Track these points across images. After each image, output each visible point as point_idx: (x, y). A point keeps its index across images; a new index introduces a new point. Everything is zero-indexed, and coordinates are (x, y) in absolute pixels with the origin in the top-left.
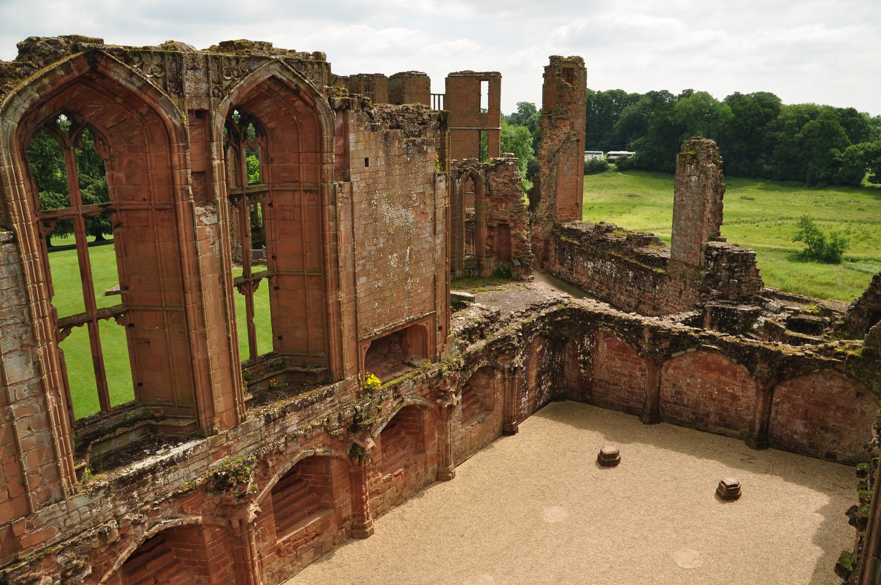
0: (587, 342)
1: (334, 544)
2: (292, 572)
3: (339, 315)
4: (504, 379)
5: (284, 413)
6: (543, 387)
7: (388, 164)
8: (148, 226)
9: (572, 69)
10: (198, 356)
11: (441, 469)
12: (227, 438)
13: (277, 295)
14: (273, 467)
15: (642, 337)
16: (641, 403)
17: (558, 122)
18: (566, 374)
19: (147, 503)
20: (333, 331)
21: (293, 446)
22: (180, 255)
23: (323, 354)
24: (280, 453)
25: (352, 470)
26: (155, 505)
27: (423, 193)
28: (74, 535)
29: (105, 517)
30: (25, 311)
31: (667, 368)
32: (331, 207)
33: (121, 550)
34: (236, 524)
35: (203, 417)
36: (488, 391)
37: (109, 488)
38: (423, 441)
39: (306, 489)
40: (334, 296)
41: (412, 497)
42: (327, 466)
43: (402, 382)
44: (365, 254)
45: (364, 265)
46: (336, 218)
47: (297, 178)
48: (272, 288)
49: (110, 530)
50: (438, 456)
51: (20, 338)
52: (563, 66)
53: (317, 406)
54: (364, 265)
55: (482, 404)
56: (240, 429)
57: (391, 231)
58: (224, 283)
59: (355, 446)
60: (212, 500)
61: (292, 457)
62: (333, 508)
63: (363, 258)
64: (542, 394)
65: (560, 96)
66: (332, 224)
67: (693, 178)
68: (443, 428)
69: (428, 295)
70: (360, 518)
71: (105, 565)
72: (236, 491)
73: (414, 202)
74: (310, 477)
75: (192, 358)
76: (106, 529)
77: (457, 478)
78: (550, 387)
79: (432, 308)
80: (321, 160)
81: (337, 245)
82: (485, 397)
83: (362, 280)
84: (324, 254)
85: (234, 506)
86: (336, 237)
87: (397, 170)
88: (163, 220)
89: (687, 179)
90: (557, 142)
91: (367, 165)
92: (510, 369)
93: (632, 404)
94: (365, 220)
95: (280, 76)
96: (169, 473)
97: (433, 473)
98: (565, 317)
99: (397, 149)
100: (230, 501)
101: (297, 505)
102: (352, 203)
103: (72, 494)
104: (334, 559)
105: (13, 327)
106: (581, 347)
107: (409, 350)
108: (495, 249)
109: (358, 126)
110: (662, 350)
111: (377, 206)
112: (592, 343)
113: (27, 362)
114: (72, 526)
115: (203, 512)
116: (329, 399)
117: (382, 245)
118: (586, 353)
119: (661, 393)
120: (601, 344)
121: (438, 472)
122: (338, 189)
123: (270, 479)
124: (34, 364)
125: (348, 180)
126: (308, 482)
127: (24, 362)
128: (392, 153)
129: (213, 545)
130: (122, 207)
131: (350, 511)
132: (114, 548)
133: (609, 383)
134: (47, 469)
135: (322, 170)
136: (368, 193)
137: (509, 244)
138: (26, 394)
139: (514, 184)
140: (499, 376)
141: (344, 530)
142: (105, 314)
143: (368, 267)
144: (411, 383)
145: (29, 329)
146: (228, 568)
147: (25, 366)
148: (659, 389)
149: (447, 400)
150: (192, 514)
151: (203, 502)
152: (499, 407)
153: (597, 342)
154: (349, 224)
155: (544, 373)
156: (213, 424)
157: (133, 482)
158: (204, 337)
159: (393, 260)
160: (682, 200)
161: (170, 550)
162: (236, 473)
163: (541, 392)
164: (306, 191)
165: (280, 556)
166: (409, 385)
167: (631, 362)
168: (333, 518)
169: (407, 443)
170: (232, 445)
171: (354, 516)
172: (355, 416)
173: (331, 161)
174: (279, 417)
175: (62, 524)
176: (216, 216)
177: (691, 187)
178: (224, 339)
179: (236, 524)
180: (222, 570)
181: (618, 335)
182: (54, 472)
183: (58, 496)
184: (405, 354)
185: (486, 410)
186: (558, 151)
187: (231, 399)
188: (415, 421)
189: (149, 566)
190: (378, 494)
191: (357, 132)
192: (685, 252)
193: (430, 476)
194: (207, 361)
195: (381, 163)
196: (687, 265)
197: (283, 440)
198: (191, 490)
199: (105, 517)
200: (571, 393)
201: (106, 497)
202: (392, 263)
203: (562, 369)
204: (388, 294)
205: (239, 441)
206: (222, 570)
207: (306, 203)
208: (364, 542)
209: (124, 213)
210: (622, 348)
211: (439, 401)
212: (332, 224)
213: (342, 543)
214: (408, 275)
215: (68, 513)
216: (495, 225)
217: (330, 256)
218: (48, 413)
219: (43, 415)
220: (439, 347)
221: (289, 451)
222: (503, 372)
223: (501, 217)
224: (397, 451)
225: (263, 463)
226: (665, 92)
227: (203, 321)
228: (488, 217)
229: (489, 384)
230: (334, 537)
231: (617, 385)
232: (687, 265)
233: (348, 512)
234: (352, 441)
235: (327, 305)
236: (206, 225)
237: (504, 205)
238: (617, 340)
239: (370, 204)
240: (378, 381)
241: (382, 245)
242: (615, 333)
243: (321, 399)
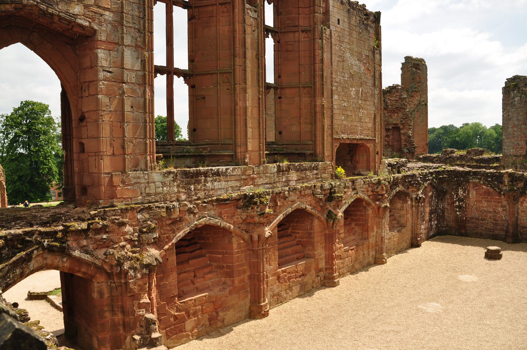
0: (461, 192)
1: (313, 288)
2: (285, 299)
3: (323, 114)
4: (412, 206)
5: (288, 169)
6: (433, 223)
8: (213, 16)
9: (418, 64)
10: (240, 104)
11: (378, 256)
12: (253, 171)
13: (280, 102)
14: (280, 206)
15: (502, 182)
16: (504, 230)
17: (413, 93)
18: (446, 217)
19: (199, 199)
20: (319, 124)
21: (293, 197)
22: (234, 31)
23: (310, 142)
24: (285, 198)
25: (327, 232)
26: (204, 202)
28: (150, 202)
29: (171, 197)
30: (142, 22)
31: (522, 203)
32: (320, 41)
33: (179, 230)
34: (256, 237)
35: (239, 150)
36: (402, 212)
37: (176, 175)
38: (367, 231)
39: (295, 242)
40: (320, 101)
41: (361, 270)
42: (312, 223)
43: (357, 179)
46: (322, 48)
47: (297, 24)
48: (277, 97)
49: (174, 207)
51: (136, 39)
52: (413, 62)
53: (308, 173)
55: (398, 222)
56: (262, 168)
58: (259, 59)
59: (330, 212)
60: (241, 215)
61: (292, 205)
62: (313, 258)
64: (432, 228)
65: (413, 79)
66: (320, 52)
67: (516, 99)
68: (379, 224)
69: (370, 125)
70: (330, 271)
71: (167, 237)
72: (259, 210)
74: (298, 233)
75: (236, 104)
76: (171, 206)
77: (388, 263)
78: (436, 225)
79: (373, 136)
80: (314, 10)
81: (323, 66)
82: (400, 217)
83: (336, 97)
84: (315, 71)
85: (255, 224)
86: (322, 60)
88: (223, 12)
89: (511, 101)
90: (413, 106)
91: (339, 24)
92: (416, 198)
93: (496, 232)
96: (215, 181)
97: (372, 257)
98: (445, 176)
100: (253, 217)
101: (289, 250)
102: (331, 43)
103: (152, 170)
104: (314, 296)
105: (133, 30)
106: (457, 196)
107: (358, 165)
108: (390, 144)
110: (518, 188)
112: (464, 192)
113: (138, 58)
114: (149, 195)
115: (234, 222)
116: (315, 172)
118: (460, 200)
119: (519, 221)
120: (471, 192)
121: (375, 258)
122: (324, 31)
123: (277, 216)
124: (142, 61)
125: (329, 28)
126: (296, 237)
127: (136, 56)
129: (238, 252)
130: (196, 5)
131: (324, 264)
132: (176, 222)
133: (479, 220)
134: (139, 142)
135: (314, 16)
137: (400, 140)
138: (134, 80)
139: (402, 101)
140: (409, 202)
141: (319, 278)
142: (179, 73)
144: (362, 183)
145: (142, 35)
146: (246, 276)
147: (136, 60)
148: (517, 218)
149: (383, 202)
150: (227, 221)
151: (234, 215)
152: (409, 225)
153: (468, 192)
154: (329, 56)
155: (433, 213)
156: (245, 158)
157: (192, 177)
158: (245, 90)
160: (509, 116)
161: (205, 256)
162: (260, 196)
163: (431, 225)
164: (302, 31)
165: (279, 282)
167: (494, 202)
168: (313, 266)
169: (356, 232)
170: (256, 179)
171: (326, 269)
172: (331, 189)
173: (319, 16)
174: (286, 171)
175: (143, 189)
176: (257, 14)
177: (515, 105)
178: (257, 98)
179: (256, 237)
181: (484, 184)
182: (142, 147)
183: (142, 166)
184: (355, 168)
185: (401, 226)
186: (414, 111)
187: (258, 144)
188: (362, 215)
189: (191, 262)
190: (341, 259)
192: (513, 148)
193: (371, 260)
194: (246, 109)
196: (516, 156)
197: (287, 188)
198: (228, 200)
199: (171, 197)
200: (453, 229)
201: (174, 181)
202: (352, 94)
203: (443, 213)
205: (260, 177)
207: (302, 39)
208: (334, 289)
210: (488, 193)
211: (377, 203)
212: (320, 52)
213: (318, 289)
215: (148, 183)
216: (391, 127)
217: (318, 73)
218: (145, 99)
219: (142, 100)
221: (290, 199)
222: (412, 200)
223: (394, 122)
224: (350, 235)
225: (274, 200)
226: (452, 126)
227: (245, 79)
228: (386, 123)
229: (403, 207)
230: (313, 282)
231: (484, 220)
232: (516, 156)
233: (322, 264)
234: (327, 208)
235: (315, 106)
236: (251, 17)
237: (396, 115)
238: (483, 188)
240: (343, 171)
242: (482, 182)
243: (311, 169)
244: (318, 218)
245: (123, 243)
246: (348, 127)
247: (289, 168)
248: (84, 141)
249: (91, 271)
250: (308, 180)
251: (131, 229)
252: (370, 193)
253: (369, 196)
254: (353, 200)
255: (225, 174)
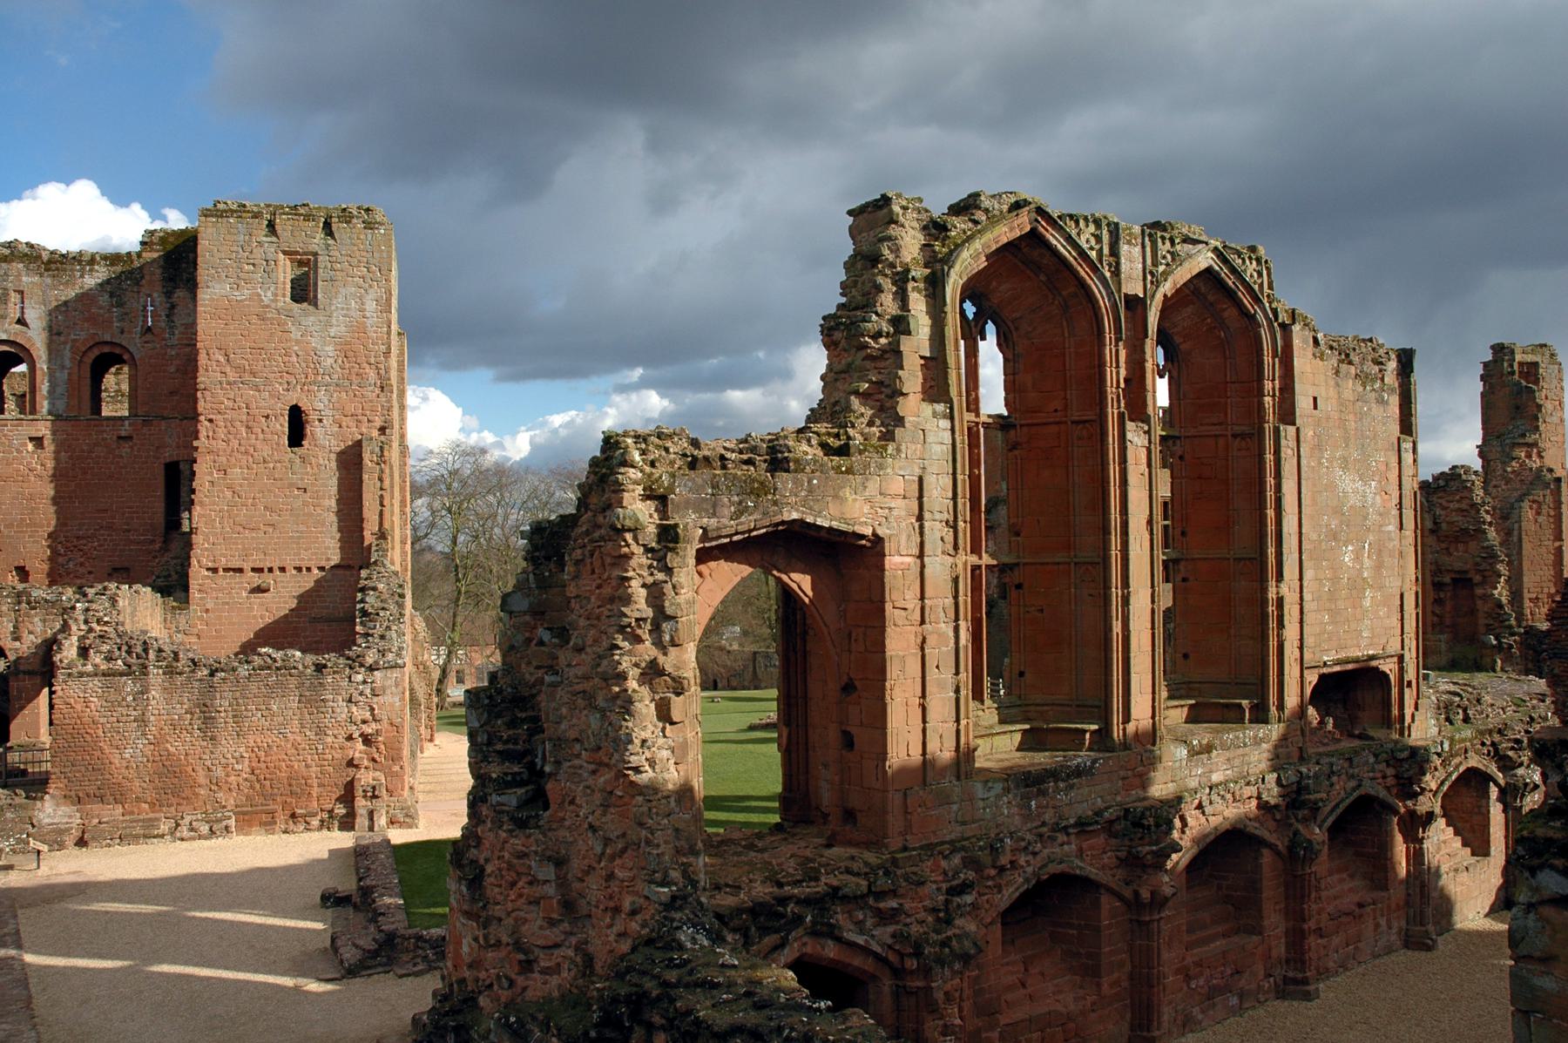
20: (1273, 643)
50: (1407, 903)
62: (1260, 933)
108: (1448, 621)
131: (1283, 949)
137: (1473, 612)
172: (1299, 783)
180: (1116, 975)
206: (1116, 975)
209: (1025, 429)
216: (1447, 579)
220: (1408, 712)
223: (1458, 565)
233: (1280, 950)
235: (1265, 602)
237: (1461, 547)
244: (1271, 846)
248: (854, 730)
249: (868, 965)
252: (1390, 781)
253: (1388, 788)
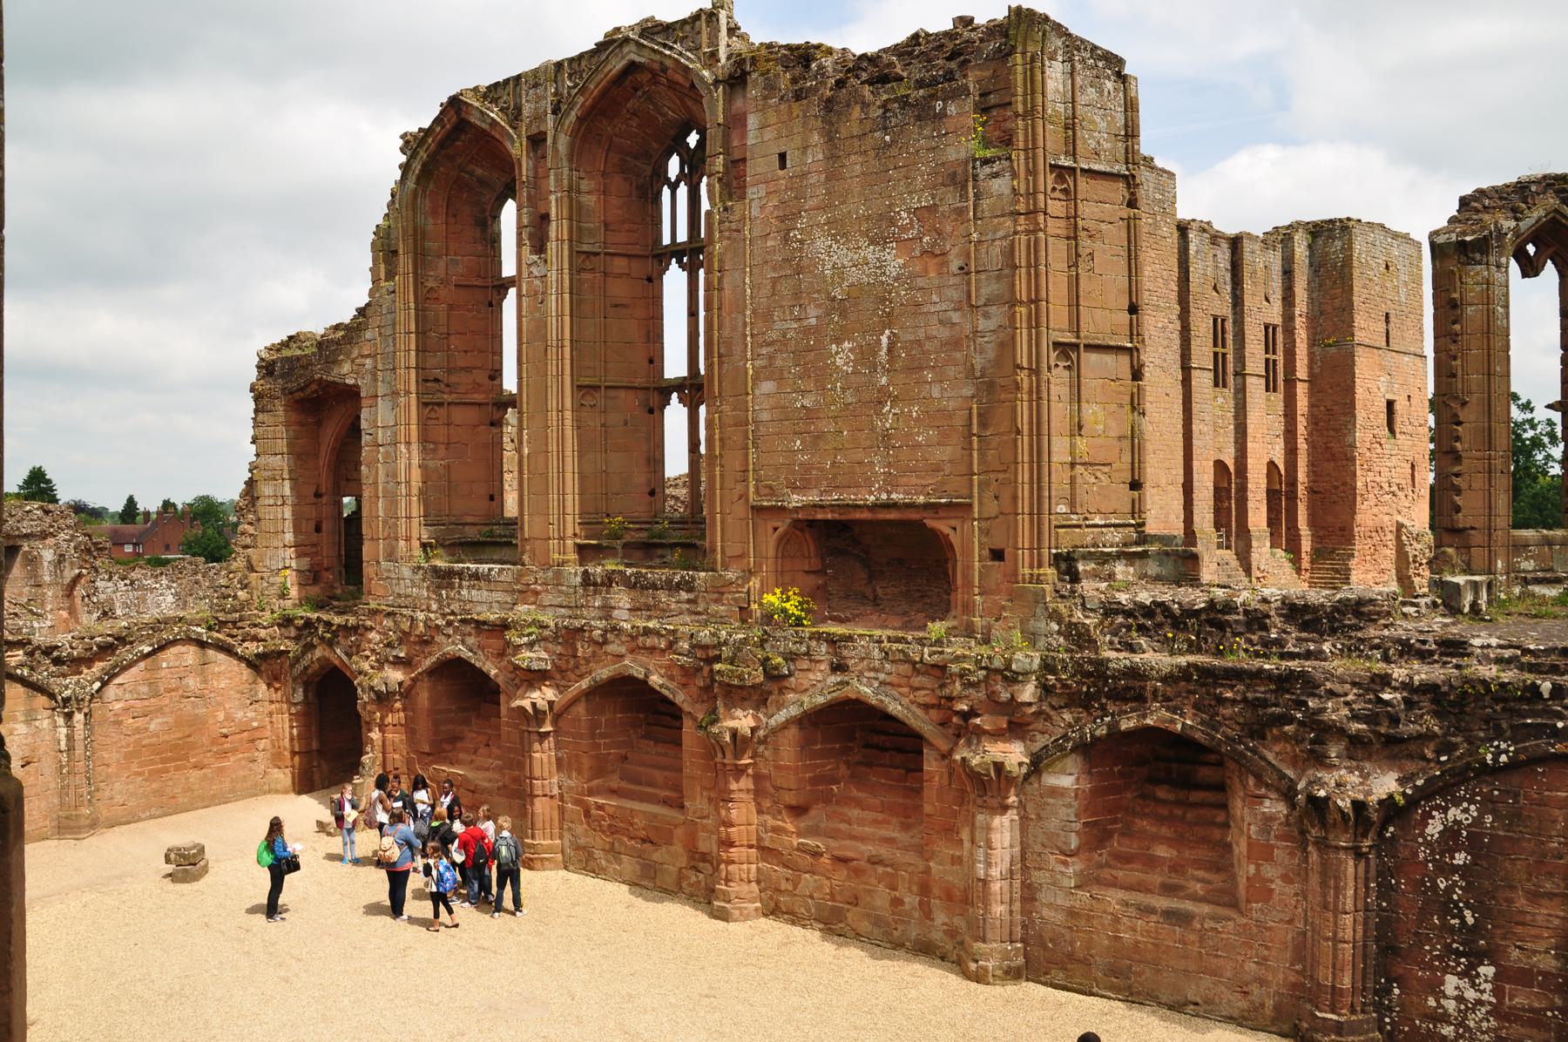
5: (609, 581)
7: (832, 157)
27: (932, 209)
43: (850, 638)
44: (774, 335)
45: (771, 358)
53: (663, 596)
54: (771, 358)
57: (838, 294)
63: (769, 344)
73: (904, 229)
87: (855, 166)
91: (783, 166)
94: (774, 269)
95: (638, 59)
96: (473, 587)
99: (855, 124)
109: (765, 98)
111: (802, 242)
114: (399, 595)
116: (684, 595)
117: (813, 321)
128: (844, 133)
136: (782, 219)
143: (779, 363)
159: (843, 356)
166: (874, 661)
174: (603, 584)
191: (762, 110)
195: (816, 156)
202: (839, 362)
204: (828, 426)
214: (882, 397)
239: (786, 240)
241: (813, 321)
245: (367, 653)
246: (822, 470)
247: (610, 581)
250: (664, 613)
251: (378, 637)
254: (820, 700)
255: (486, 578)
